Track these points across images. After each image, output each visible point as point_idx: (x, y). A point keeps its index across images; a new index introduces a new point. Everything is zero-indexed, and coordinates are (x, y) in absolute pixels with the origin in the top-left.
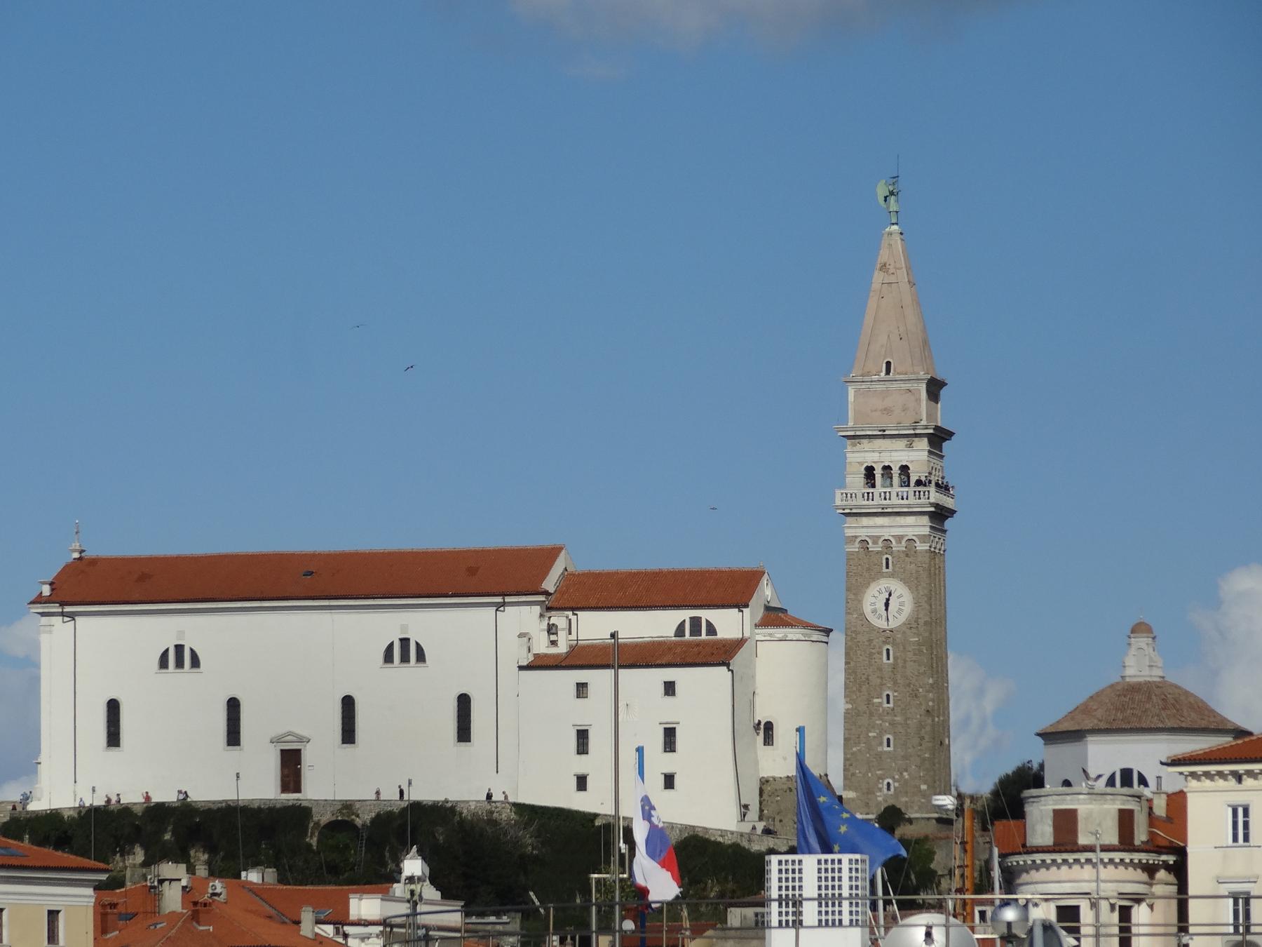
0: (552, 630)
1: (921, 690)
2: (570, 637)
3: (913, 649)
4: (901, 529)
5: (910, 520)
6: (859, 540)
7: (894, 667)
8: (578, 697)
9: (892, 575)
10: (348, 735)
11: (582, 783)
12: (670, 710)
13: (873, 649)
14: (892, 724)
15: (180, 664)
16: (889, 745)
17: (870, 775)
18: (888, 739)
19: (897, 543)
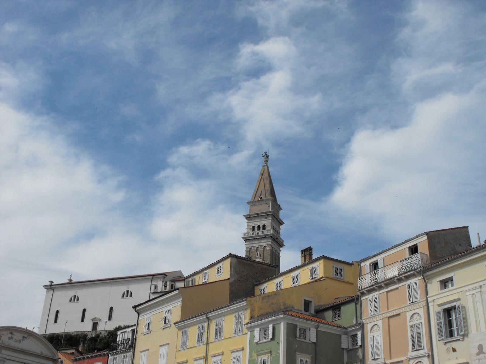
4: (262, 244)
5: (265, 240)
6: (250, 248)
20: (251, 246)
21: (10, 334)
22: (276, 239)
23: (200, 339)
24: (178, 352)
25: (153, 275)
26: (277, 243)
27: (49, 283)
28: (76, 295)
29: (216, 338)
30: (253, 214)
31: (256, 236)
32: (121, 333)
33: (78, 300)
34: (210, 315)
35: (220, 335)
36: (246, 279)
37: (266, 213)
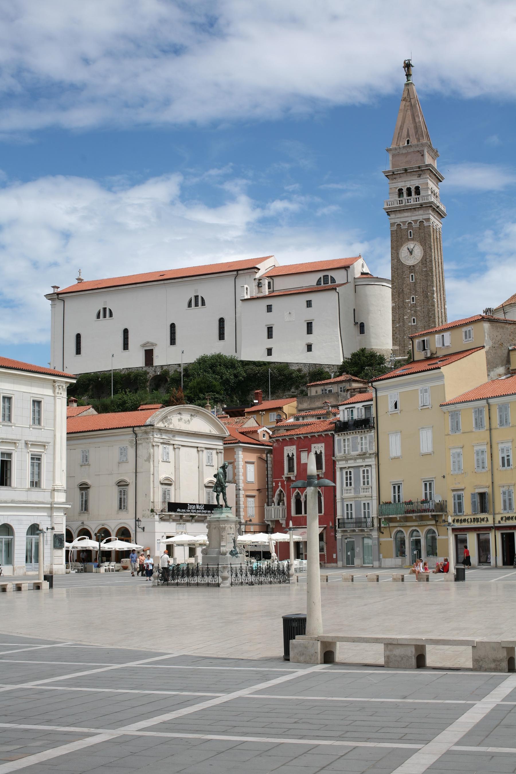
0: (259, 285)
1: (429, 294)
2: (270, 290)
3: (425, 274)
4: (416, 217)
5: (421, 212)
7: (415, 284)
8: (268, 312)
9: (413, 240)
10: (173, 341)
11: (269, 352)
12: (309, 314)
13: (405, 276)
14: (415, 312)
15: (105, 316)
16: (414, 322)
17: (405, 337)
18: (414, 319)
19: (415, 223)
20: (398, 221)
21: (179, 415)
22: (437, 208)
23: (479, 424)
24: (448, 437)
25: (237, 271)
26: (437, 213)
27: (51, 291)
28: (105, 307)
29: (501, 424)
30: (398, 170)
31: (405, 206)
32: (346, 408)
33: (111, 315)
34: (490, 401)
35: (506, 422)
36: (500, 345)
37: (419, 167)
